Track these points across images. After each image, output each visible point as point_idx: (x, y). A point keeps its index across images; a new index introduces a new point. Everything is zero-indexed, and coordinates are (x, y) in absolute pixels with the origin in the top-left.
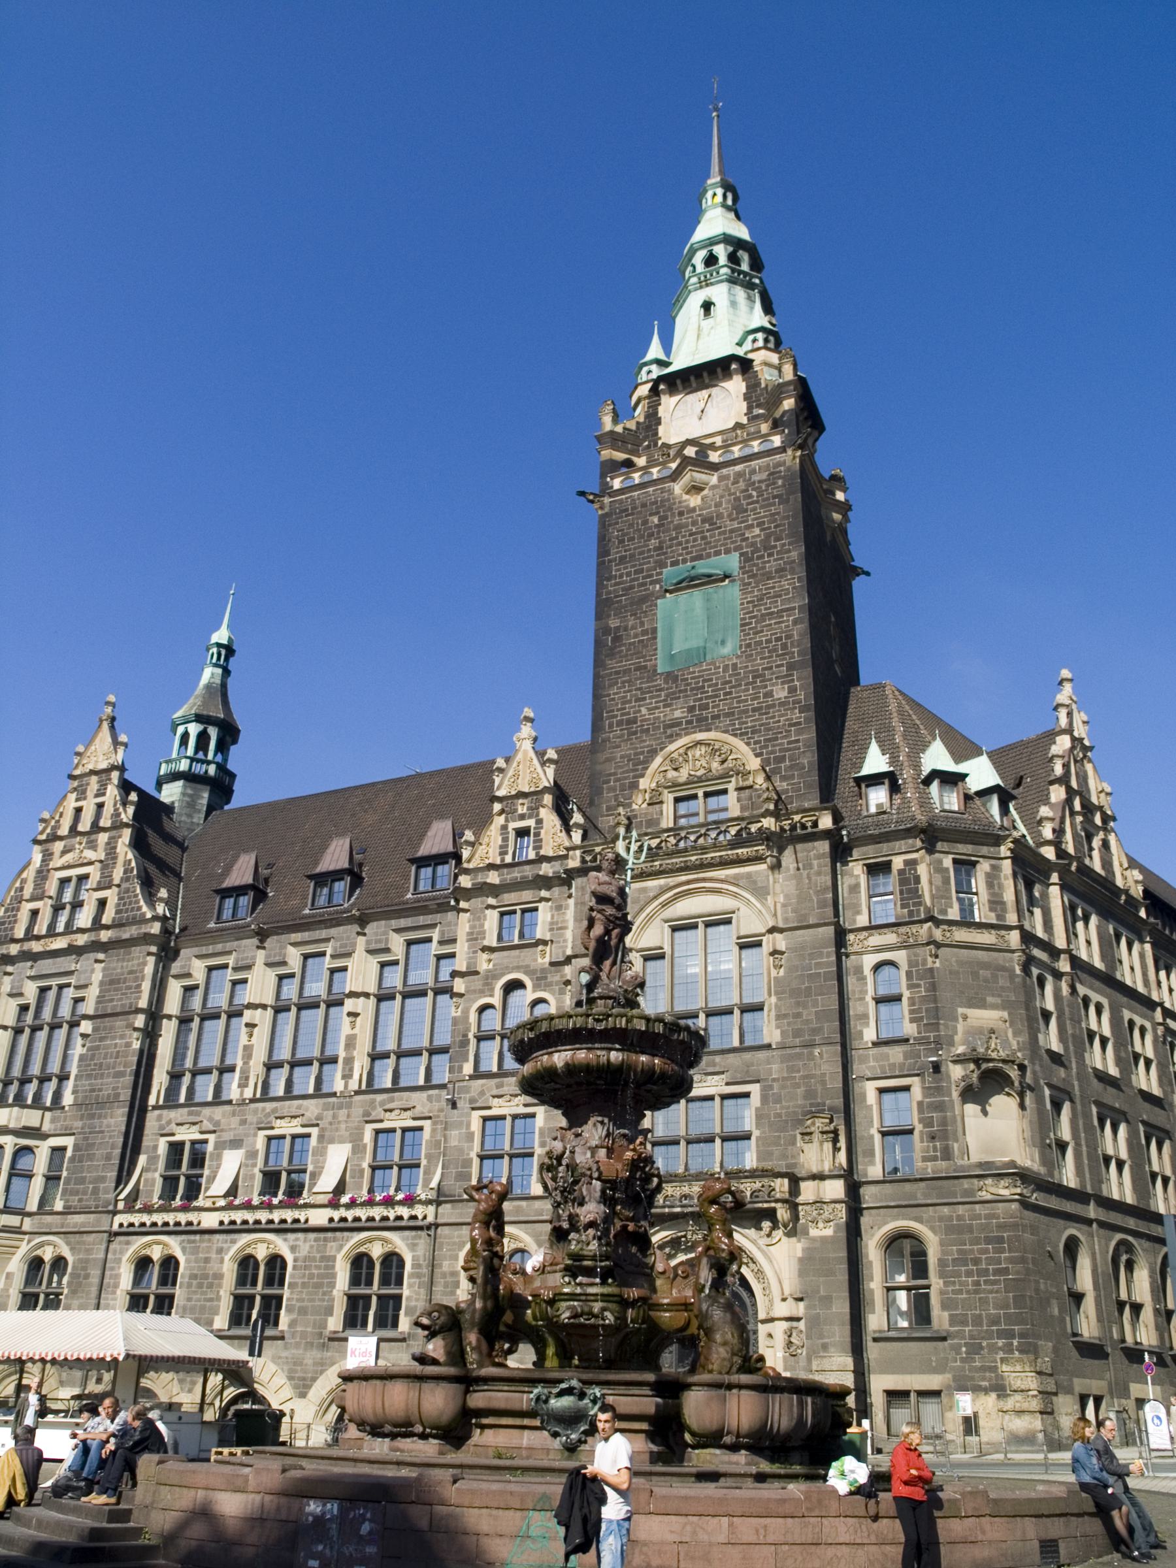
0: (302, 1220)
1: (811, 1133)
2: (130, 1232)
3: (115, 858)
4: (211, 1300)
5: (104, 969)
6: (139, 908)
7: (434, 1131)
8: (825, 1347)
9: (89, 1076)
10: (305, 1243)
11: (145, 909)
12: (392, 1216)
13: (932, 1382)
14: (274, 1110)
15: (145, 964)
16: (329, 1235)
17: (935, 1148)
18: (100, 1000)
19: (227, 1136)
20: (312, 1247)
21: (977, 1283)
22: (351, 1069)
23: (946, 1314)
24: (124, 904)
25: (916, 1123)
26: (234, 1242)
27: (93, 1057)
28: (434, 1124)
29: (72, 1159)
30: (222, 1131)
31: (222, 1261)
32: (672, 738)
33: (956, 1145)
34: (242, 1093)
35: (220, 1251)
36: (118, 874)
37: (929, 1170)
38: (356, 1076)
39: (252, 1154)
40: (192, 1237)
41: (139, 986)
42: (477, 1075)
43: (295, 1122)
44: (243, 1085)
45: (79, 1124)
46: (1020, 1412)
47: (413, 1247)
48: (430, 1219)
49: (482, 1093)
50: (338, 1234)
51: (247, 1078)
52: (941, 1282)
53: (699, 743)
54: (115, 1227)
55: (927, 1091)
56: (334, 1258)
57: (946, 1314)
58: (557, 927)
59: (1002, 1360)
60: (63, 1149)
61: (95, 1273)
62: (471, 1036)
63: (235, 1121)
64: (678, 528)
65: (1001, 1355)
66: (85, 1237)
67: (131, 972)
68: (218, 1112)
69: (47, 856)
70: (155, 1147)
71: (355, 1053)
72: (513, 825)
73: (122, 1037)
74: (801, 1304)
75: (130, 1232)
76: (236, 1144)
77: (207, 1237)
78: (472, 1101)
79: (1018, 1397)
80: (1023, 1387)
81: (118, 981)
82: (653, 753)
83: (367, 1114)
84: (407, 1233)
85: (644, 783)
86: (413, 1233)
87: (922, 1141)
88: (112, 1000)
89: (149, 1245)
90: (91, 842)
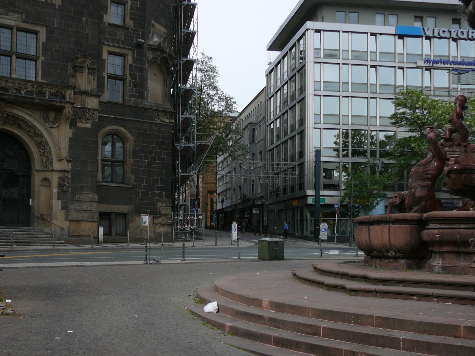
1: (83, 67)
8: (82, 188)
13: (124, 209)
17: (136, 92)
21: (149, 163)
23: (134, 176)
25: (128, 76)
33: (145, 92)
37: (132, 102)
46: (163, 225)
52: (133, 160)
57: (134, 176)
59: (157, 201)
65: (157, 198)
74: (70, 164)
79: (163, 218)
80: (166, 213)
87: (130, 86)
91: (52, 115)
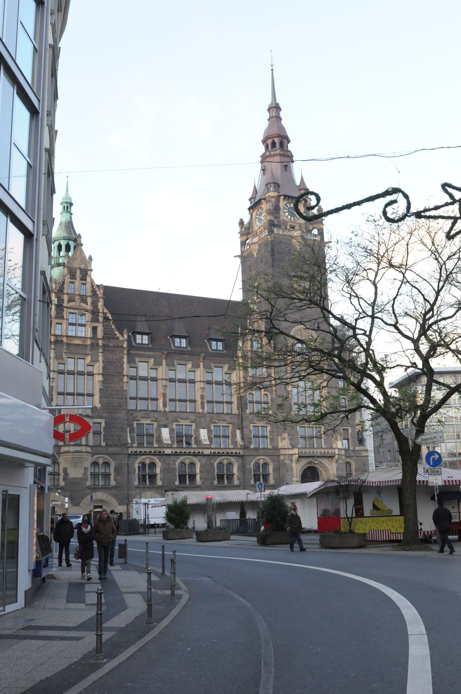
0: (201, 452)
2: (136, 454)
4: (173, 476)
5: (103, 356)
6: (116, 335)
7: (233, 428)
9: (106, 397)
10: (204, 460)
11: (118, 335)
12: (230, 452)
14: (179, 416)
15: (123, 358)
16: (211, 457)
18: (104, 368)
19: (162, 423)
20: (206, 460)
22: (204, 406)
24: (107, 331)
26: (179, 458)
27: (106, 390)
28: (233, 425)
29: (105, 428)
30: (159, 421)
31: (175, 464)
34: (165, 409)
35: (174, 461)
38: (206, 408)
39: (171, 431)
40: (162, 456)
41: (122, 366)
43: (187, 421)
44: (165, 405)
45: (106, 415)
47: (237, 461)
48: (242, 453)
49: (253, 419)
50: (214, 457)
51: (166, 404)
54: (130, 452)
55: (352, 430)
56: (214, 464)
60: (100, 423)
61: (125, 468)
62: (248, 402)
63: (164, 419)
66: (118, 456)
67: (117, 360)
68: (156, 415)
70: (133, 425)
71: (205, 401)
73: (119, 384)
75: (136, 454)
76: (165, 426)
77: (168, 456)
78: (250, 421)
81: (112, 362)
83: (211, 420)
84: (235, 457)
86: (237, 457)
88: (111, 369)
89: (145, 459)
90: (84, 300)
91: (330, 459)
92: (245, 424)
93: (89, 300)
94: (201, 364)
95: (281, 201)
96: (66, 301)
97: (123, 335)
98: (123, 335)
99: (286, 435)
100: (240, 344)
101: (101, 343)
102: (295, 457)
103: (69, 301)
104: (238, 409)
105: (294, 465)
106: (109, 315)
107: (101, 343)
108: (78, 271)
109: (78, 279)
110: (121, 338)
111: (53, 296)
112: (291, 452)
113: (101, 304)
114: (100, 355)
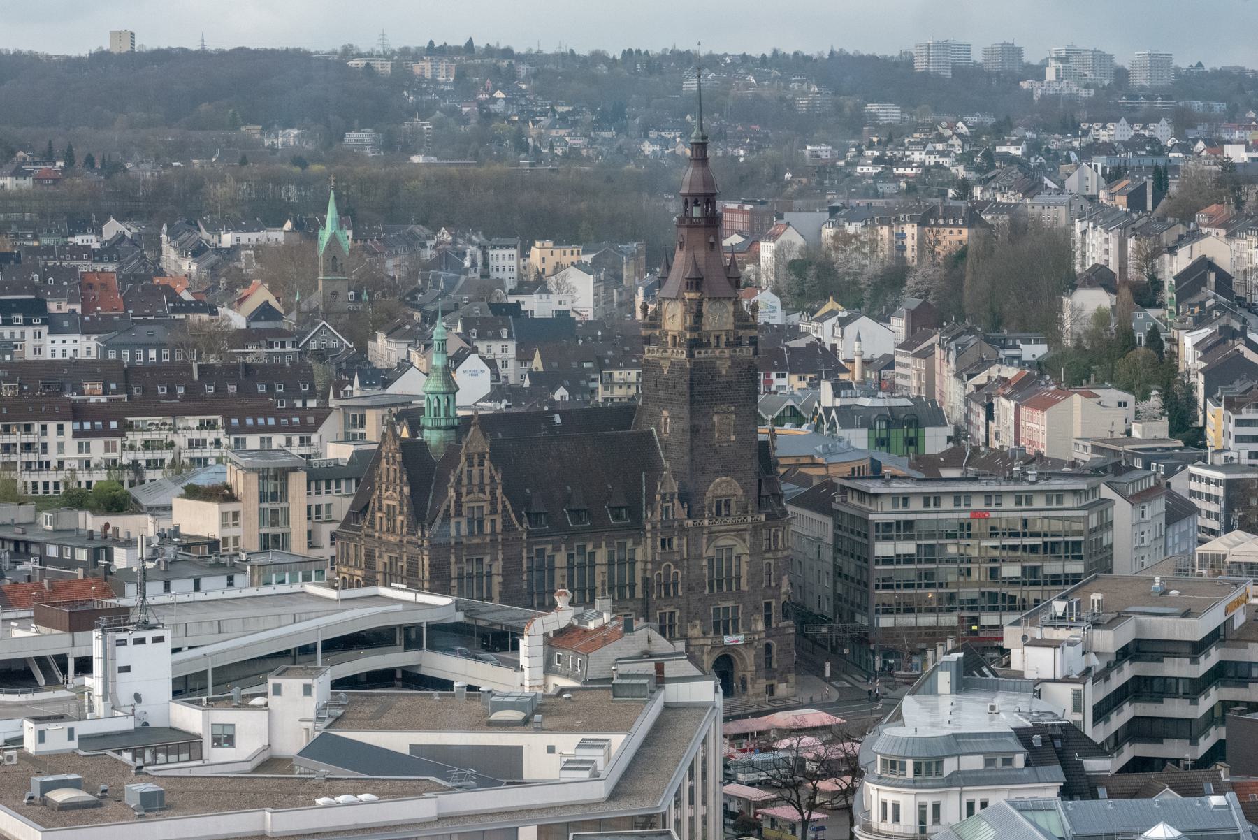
3: (497, 499)
32: (716, 477)
36: (500, 507)
42: (659, 597)
53: (725, 481)
58: (680, 546)
64: (719, 382)
69: (459, 494)
72: (665, 505)
82: (711, 482)
85: (708, 495)
92: (650, 611)
93: (487, 489)
94: (604, 543)
95: (705, 304)
96: (464, 494)
97: (522, 526)
98: (522, 526)
99: (698, 622)
100: (649, 515)
101: (500, 537)
102: (707, 649)
103: (468, 494)
104: (643, 592)
105: (705, 657)
106: (507, 503)
107: (500, 537)
108: (476, 457)
109: (476, 465)
110: (520, 529)
111: (452, 493)
112: (702, 642)
113: (499, 492)
114: (500, 552)
